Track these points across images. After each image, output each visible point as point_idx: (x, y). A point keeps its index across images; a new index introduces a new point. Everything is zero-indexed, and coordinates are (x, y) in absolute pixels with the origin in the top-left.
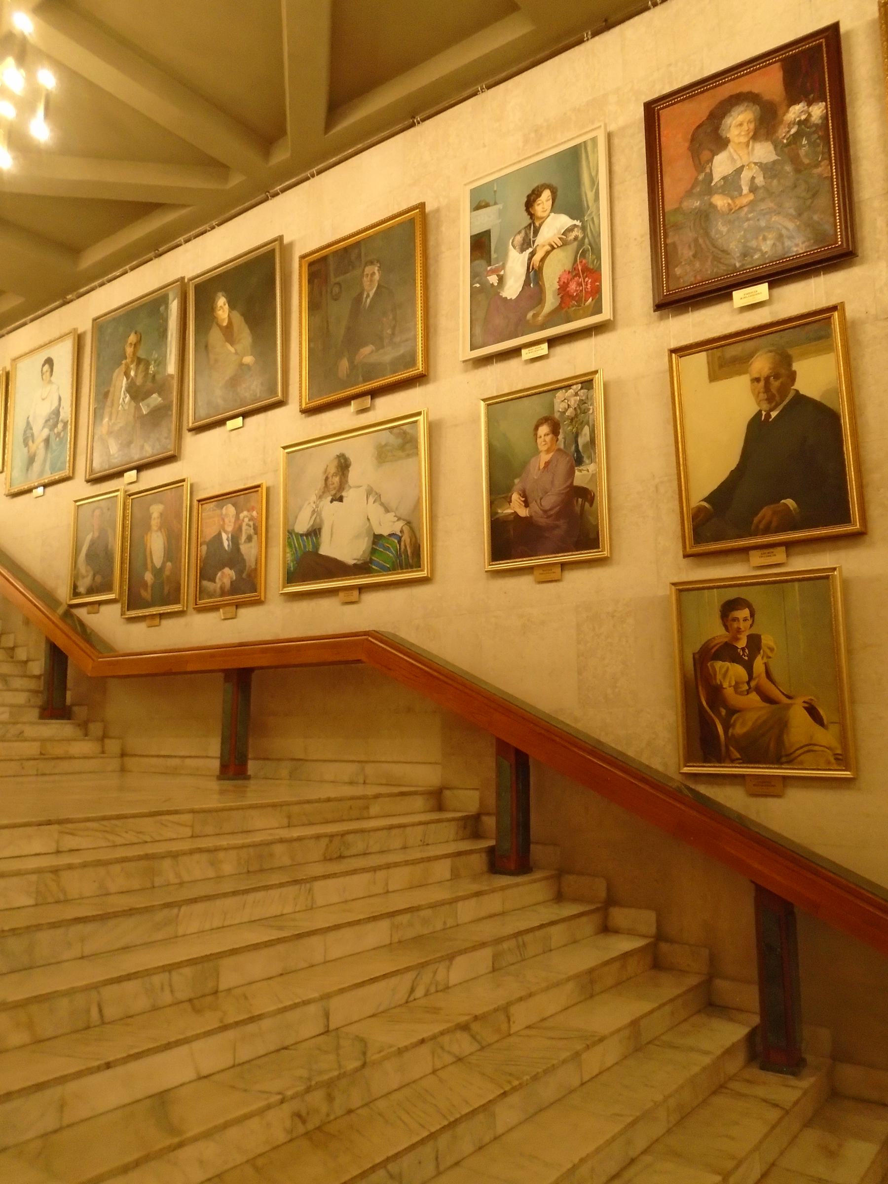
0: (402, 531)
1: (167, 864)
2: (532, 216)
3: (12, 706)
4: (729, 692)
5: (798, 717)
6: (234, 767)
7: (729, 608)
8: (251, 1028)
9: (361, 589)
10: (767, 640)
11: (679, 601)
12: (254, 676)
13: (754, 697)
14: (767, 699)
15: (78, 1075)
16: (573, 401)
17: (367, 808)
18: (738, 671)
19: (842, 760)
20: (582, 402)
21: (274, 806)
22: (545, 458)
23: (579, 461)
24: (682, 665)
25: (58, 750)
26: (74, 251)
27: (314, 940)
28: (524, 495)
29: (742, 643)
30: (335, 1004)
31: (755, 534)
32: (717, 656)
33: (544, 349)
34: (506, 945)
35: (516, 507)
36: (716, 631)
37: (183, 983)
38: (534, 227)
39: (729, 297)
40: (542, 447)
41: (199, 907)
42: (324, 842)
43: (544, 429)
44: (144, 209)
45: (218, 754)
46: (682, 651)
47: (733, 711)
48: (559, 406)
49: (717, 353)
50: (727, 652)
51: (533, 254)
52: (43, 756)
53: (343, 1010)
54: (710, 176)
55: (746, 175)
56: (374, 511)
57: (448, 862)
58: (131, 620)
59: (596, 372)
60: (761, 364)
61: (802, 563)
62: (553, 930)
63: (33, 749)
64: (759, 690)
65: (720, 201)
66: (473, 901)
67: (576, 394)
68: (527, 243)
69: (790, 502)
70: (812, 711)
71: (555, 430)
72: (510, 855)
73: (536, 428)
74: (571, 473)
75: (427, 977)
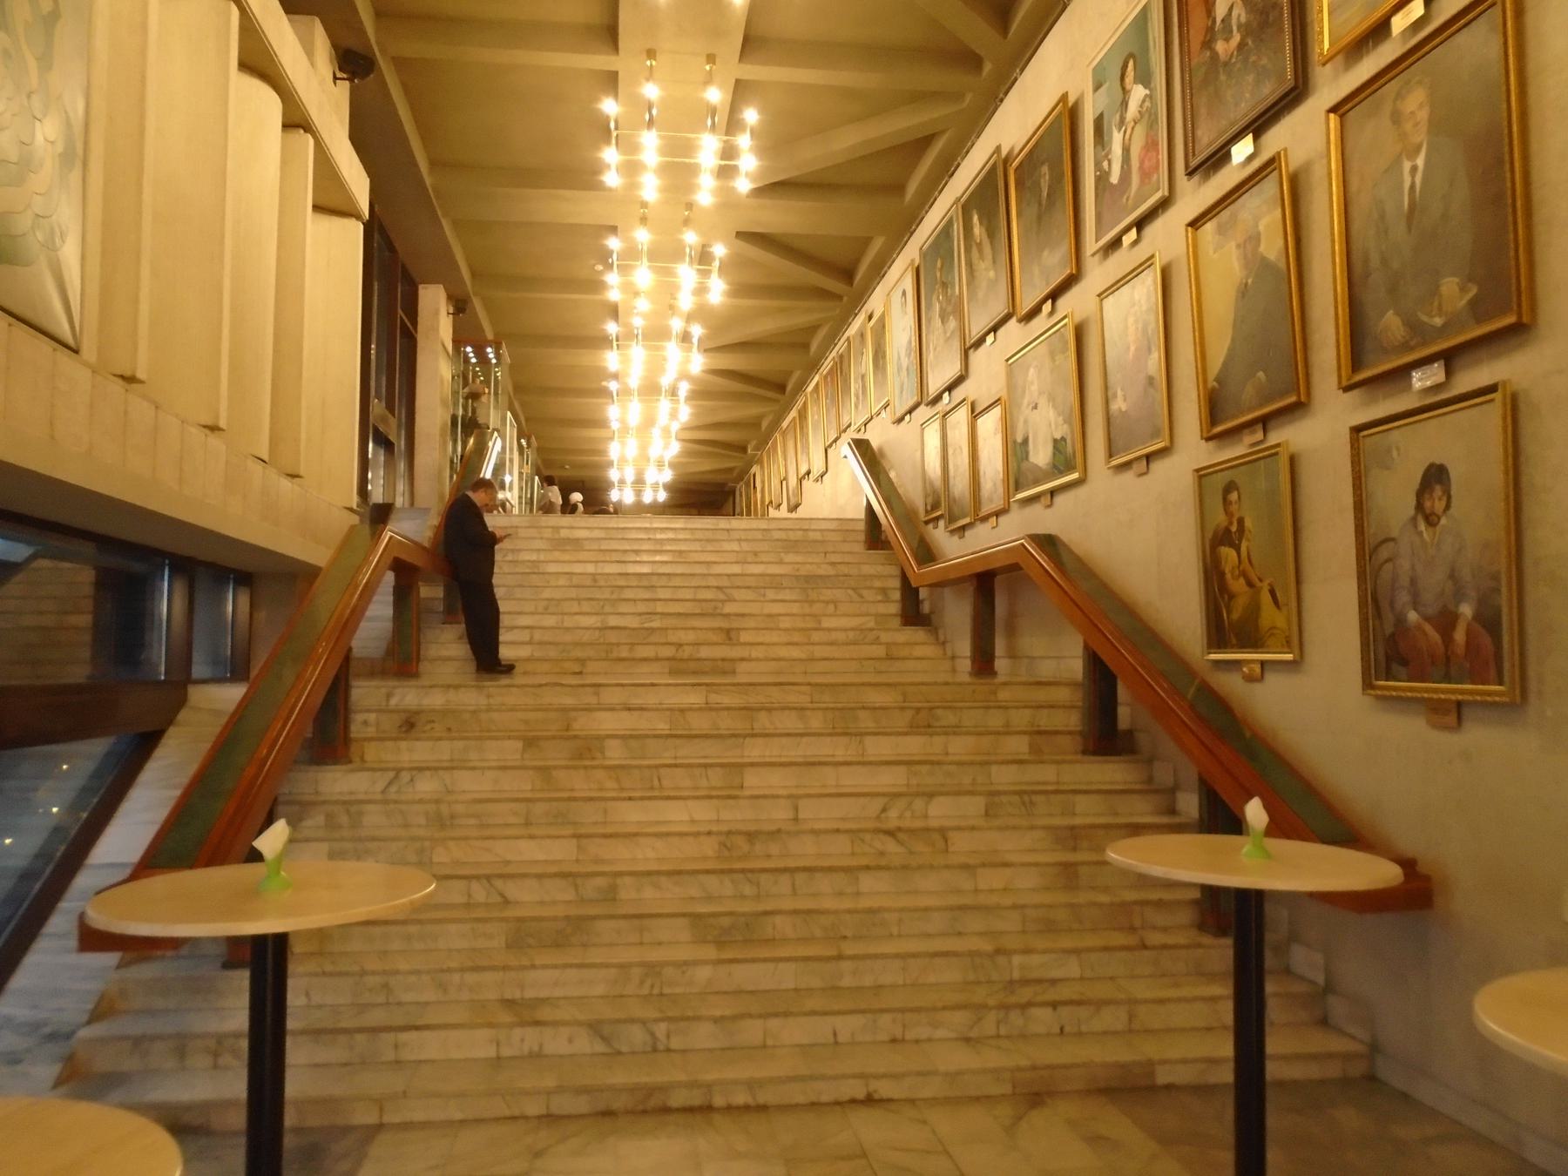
1: (763, 714)
2: (1123, 89)
3: (877, 615)
4: (1228, 576)
5: (1266, 598)
6: (983, 662)
7: (1229, 488)
8: (731, 802)
9: (1053, 492)
10: (1248, 523)
11: (1200, 486)
12: (999, 581)
13: (1242, 580)
14: (1250, 584)
15: (614, 799)
17: (995, 693)
18: (1232, 553)
19: (1287, 645)
21: (888, 685)
24: (1204, 552)
25: (904, 652)
26: (899, 188)
27: (828, 770)
29: (1234, 528)
30: (802, 803)
31: (1242, 413)
32: (1222, 543)
33: (1133, 233)
34: (1004, 799)
36: (1218, 518)
37: (716, 778)
38: (1124, 104)
39: (1227, 157)
41: (760, 741)
42: (909, 714)
44: (925, 142)
45: (968, 654)
46: (1203, 537)
47: (1232, 597)
49: (1215, 221)
52: (889, 657)
53: (807, 810)
54: (1214, 21)
55: (1235, 13)
56: (1051, 414)
57: (1025, 740)
58: (952, 532)
59: (1153, 256)
62: (1079, 798)
63: (880, 651)
64: (1244, 574)
66: (1014, 767)
68: (1122, 121)
69: (1261, 374)
70: (1272, 593)
72: (1105, 736)
75: (901, 803)
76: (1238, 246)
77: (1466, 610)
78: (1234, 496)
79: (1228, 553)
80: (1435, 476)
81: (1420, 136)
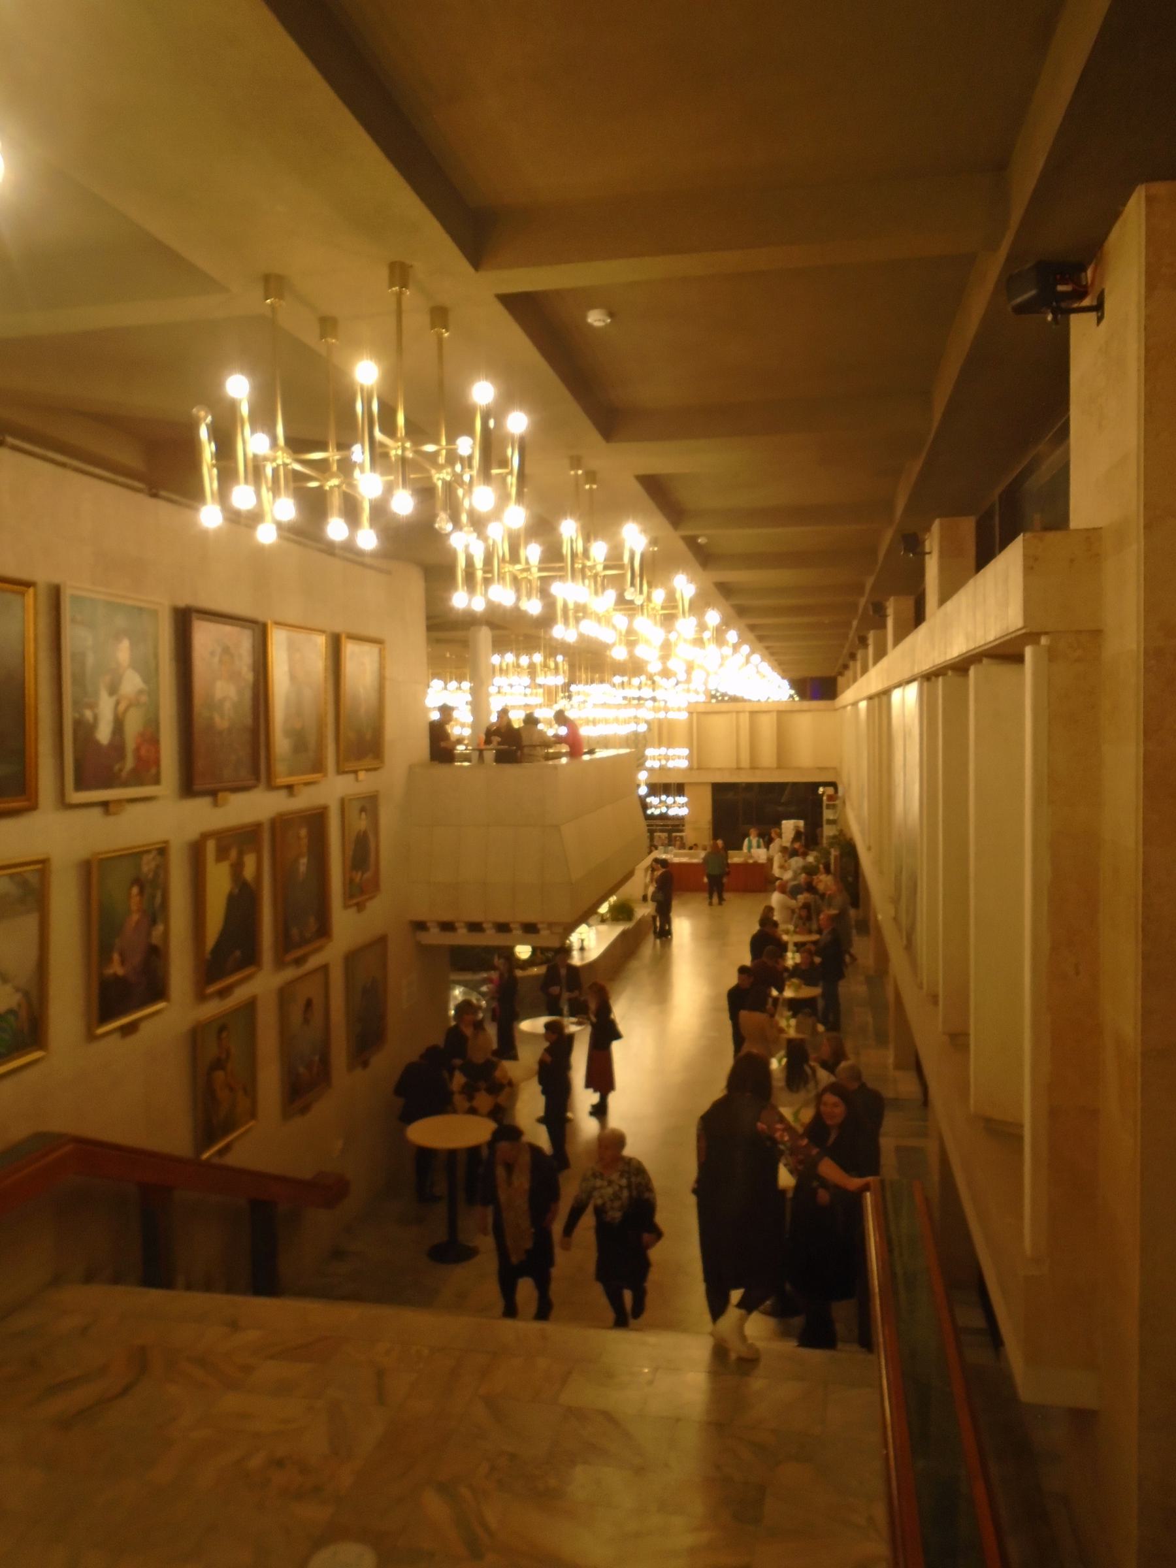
0: (19, 1005)
16: (153, 865)
20: (158, 867)
22: (135, 917)
23: (154, 922)
28: (121, 955)
35: (116, 968)
40: (134, 907)
43: (135, 890)
48: (145, 869)
50: (218, 1064)
51: (118, 703)
60: (233, 853)
61: (241, 994)
65: (217, 719)
67: (154, 859)
71: (141, 892)
73: (130, 889)
74: (149, 934)
76: (232, 865)
77: (317, 1058)
78: (224, 1035)
79: (220, 1075)
80: (309, 1004)
81: (305, 849)
